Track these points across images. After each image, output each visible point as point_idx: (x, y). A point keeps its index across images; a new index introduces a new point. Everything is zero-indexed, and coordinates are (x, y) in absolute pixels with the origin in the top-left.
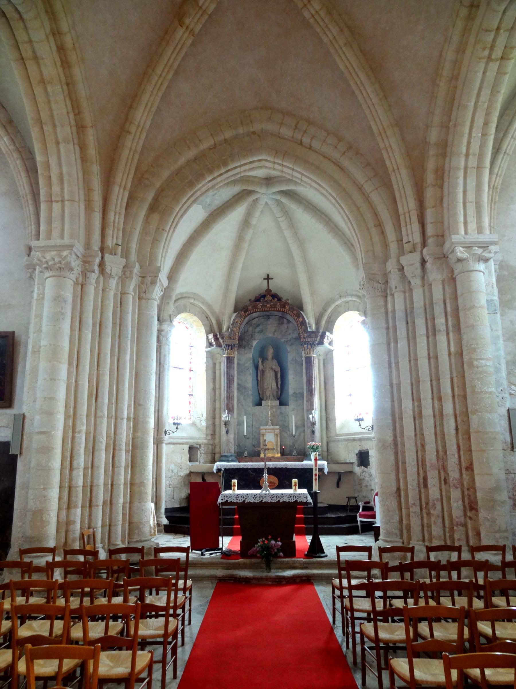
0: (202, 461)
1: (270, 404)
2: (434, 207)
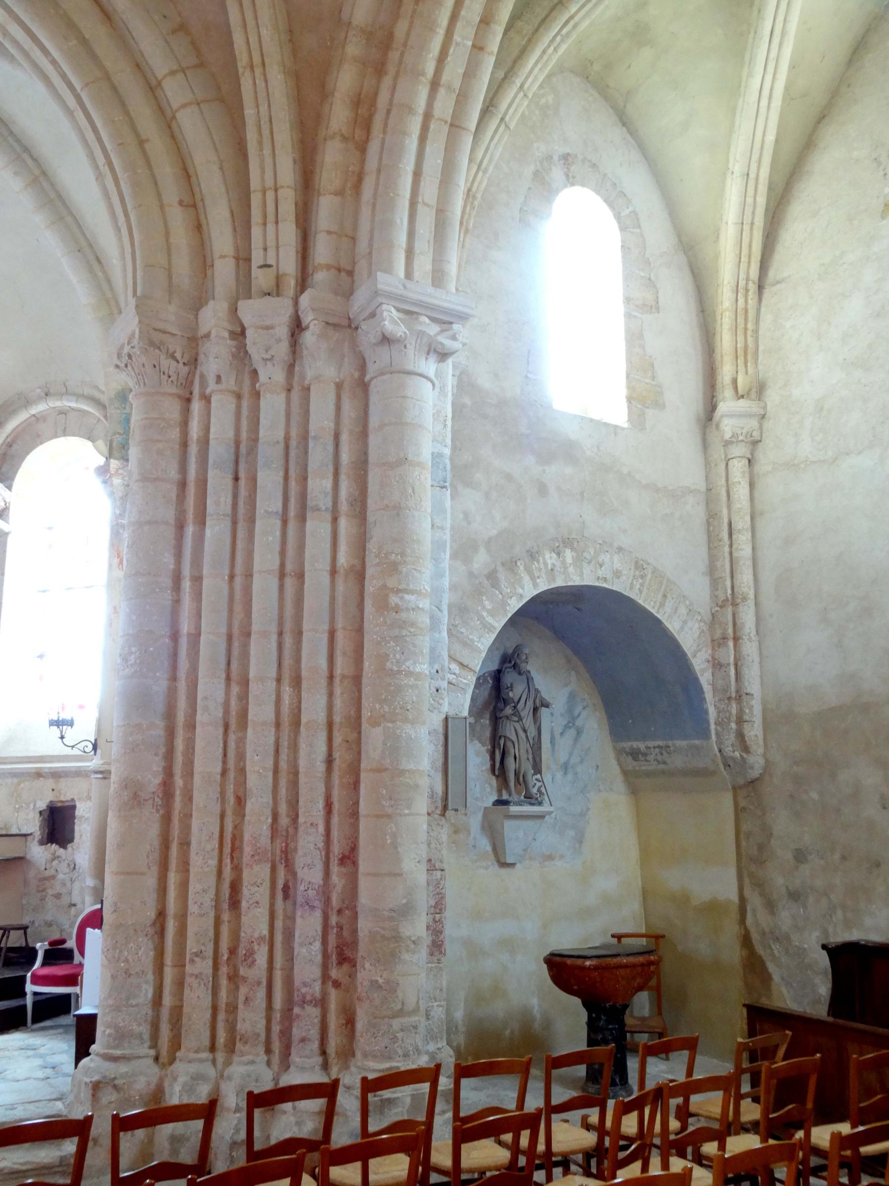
2: (340, 193)
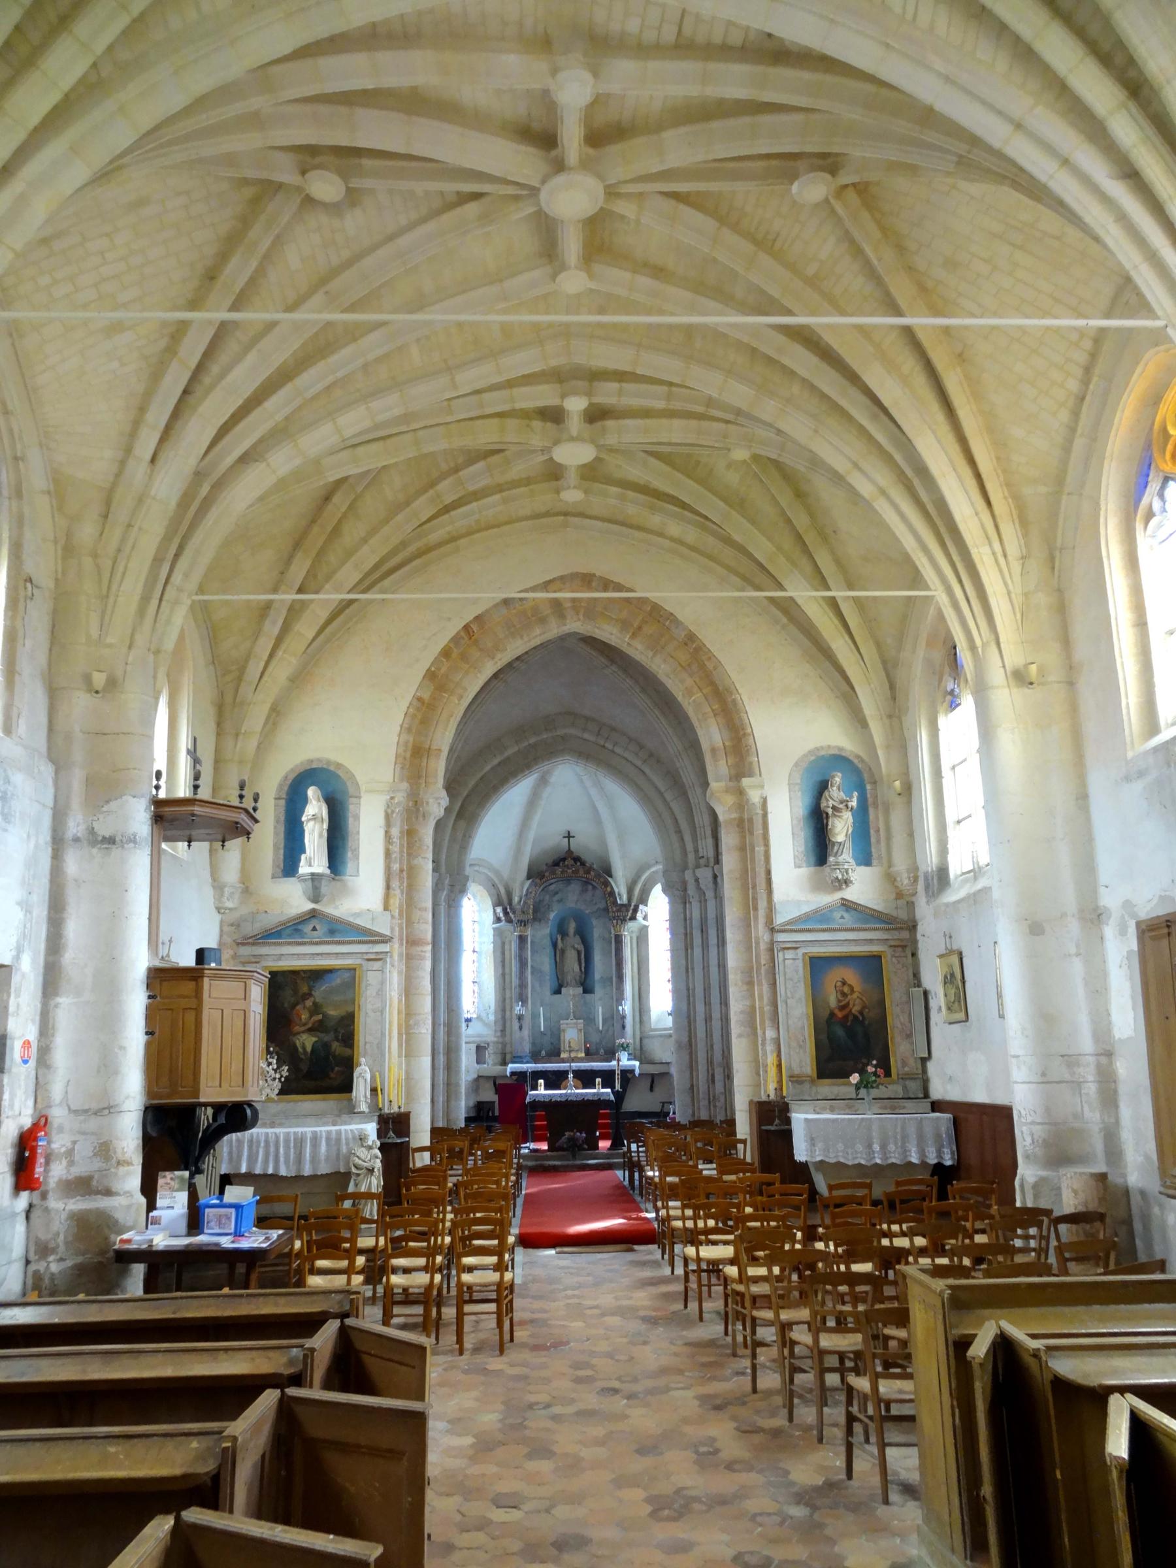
1: (572, 992)
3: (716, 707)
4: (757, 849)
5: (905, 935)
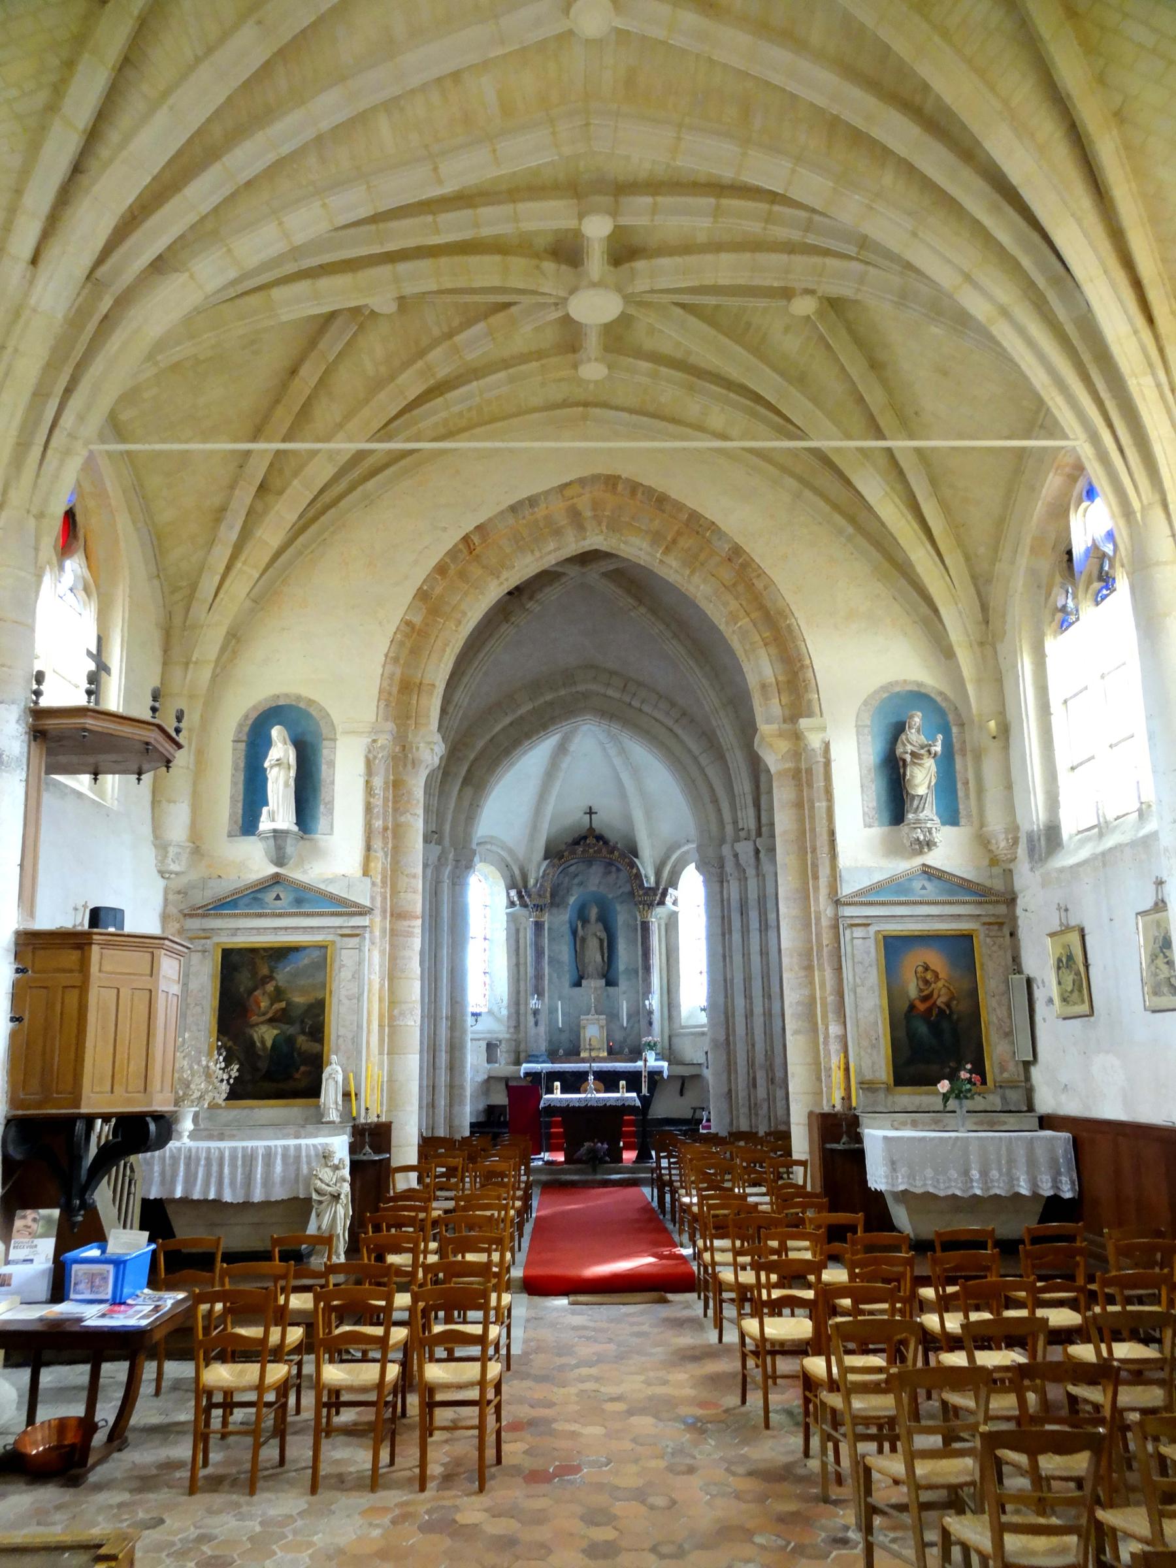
0: (503, 1062)
1: (593, 985)
3: (767, 634)
4: (817, 804)
5: (1002, 909)
